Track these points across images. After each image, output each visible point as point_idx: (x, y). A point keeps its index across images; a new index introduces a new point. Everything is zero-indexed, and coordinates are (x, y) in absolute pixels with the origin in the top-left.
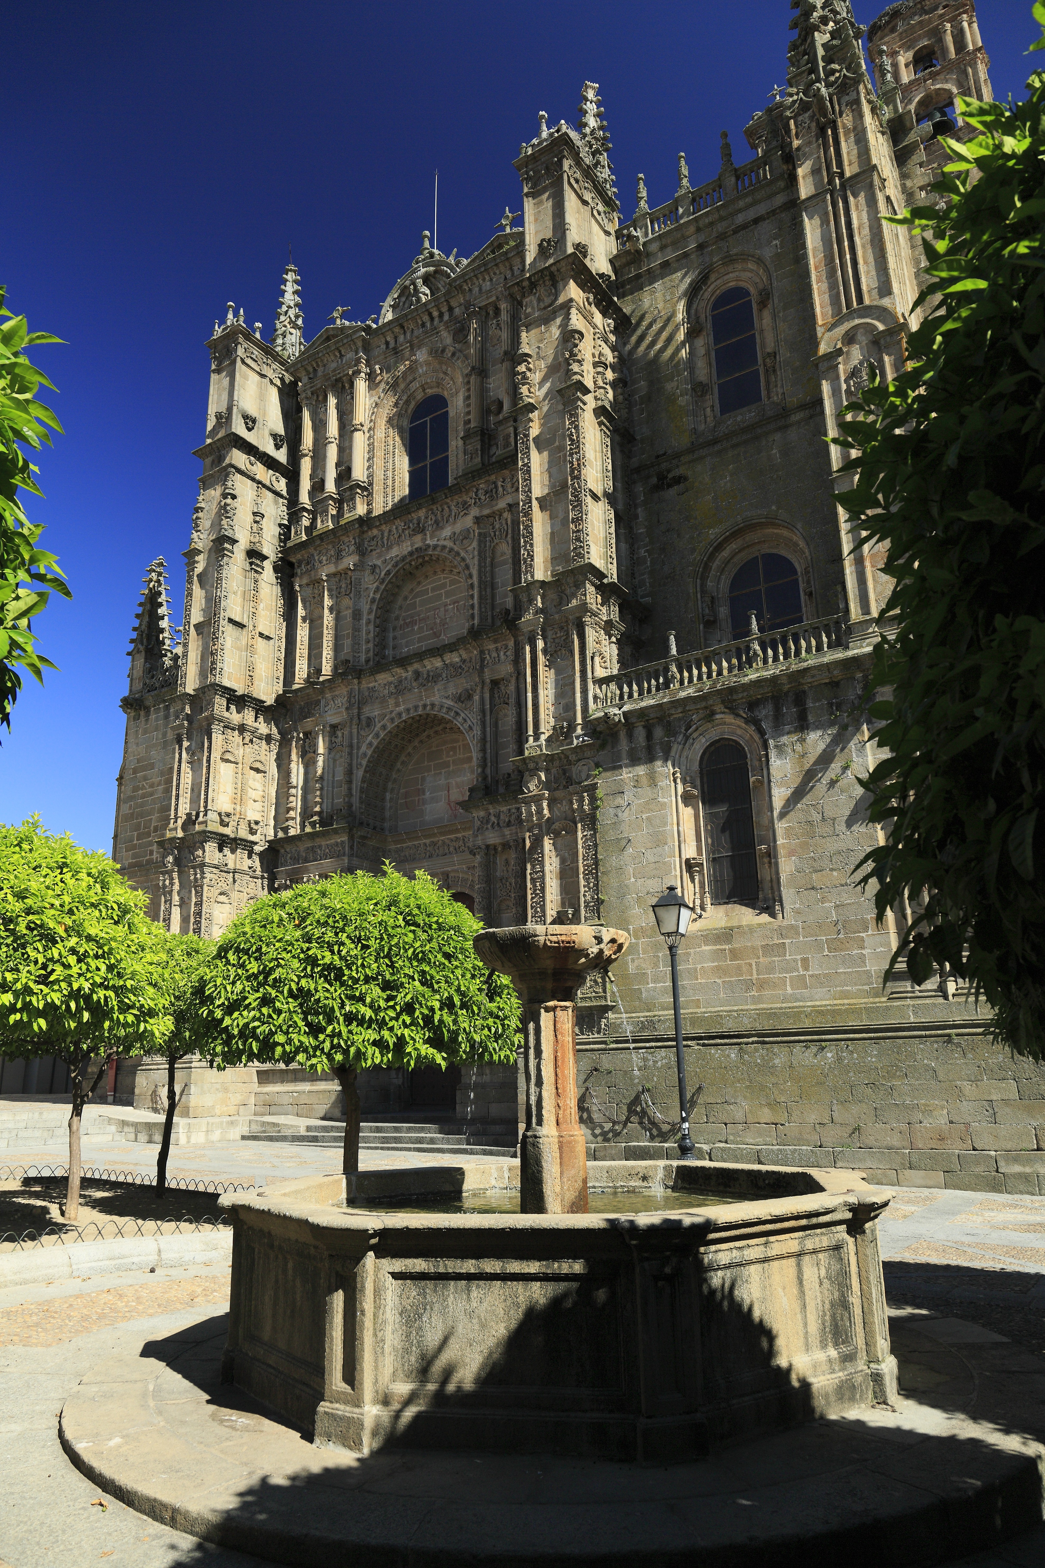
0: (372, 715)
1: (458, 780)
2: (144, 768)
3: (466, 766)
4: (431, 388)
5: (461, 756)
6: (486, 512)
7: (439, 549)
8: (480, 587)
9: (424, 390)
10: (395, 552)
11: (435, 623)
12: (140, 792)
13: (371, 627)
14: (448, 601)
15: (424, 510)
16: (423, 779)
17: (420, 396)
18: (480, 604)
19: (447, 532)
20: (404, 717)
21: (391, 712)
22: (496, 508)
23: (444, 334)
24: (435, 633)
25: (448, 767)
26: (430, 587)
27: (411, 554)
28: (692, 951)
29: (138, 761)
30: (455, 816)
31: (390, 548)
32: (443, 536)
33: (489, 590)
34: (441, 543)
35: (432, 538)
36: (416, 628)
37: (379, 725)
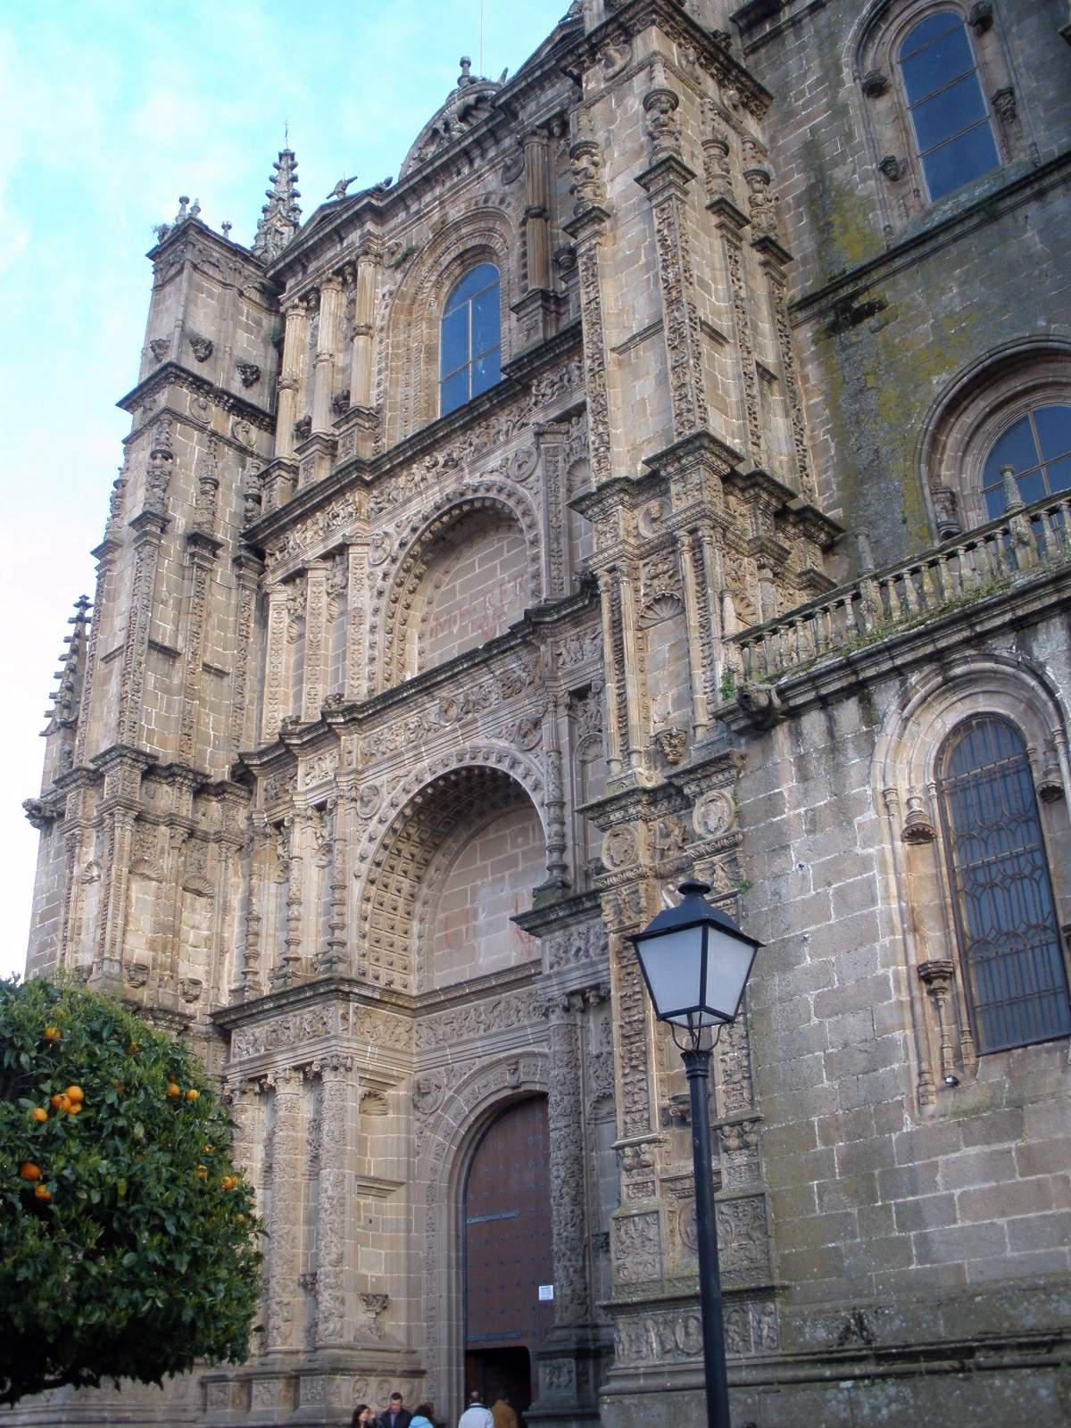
0: (377, 783)
6: (555, 413)
7: (482, 489)
8: (548, 536)
11: (485, 617)
13: (380, 637)
14: (506, 576)
16: (474, 891)
18: (549, 564)
19: (494, 461)
22: (570, 405)
23: (489, 177)
25: (516, 865)
28: (941, 1159)
32: (489, 468)
33: (564, 541)
34: (487, 478)
35: (471, 473)
36: (455, 629)
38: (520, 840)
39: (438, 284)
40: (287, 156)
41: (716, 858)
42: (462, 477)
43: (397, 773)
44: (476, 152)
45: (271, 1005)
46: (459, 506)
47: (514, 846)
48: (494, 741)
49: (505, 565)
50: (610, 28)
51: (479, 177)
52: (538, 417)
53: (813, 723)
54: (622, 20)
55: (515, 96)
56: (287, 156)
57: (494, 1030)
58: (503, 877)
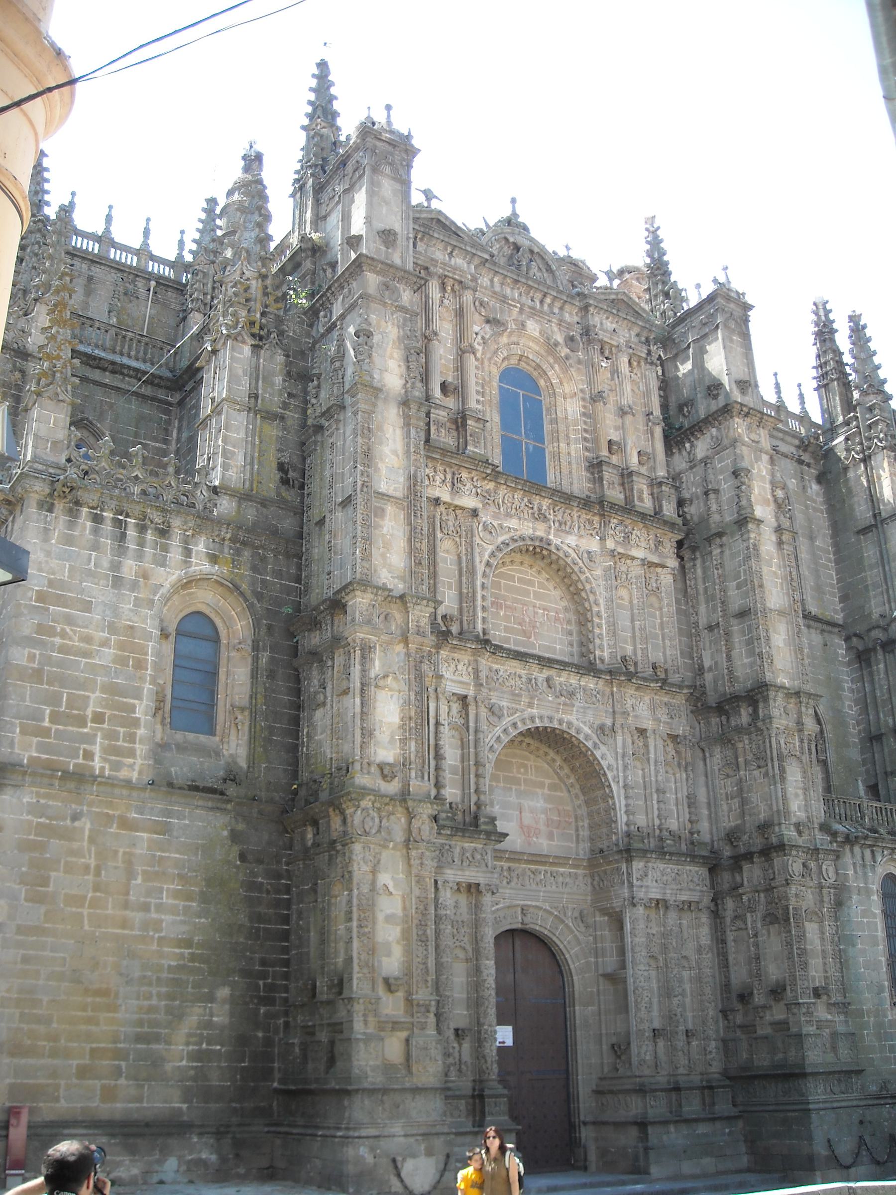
1: (531, 803)
2: (61, 601)
3: (539, 791)
4: (528, 364)
5: (533, 778)
9: (520, 360)
10: (513, 523)
11: (523, 619)
12: (58, 640)
14: (538, 603)
15: (550, 501)
17: (514, 361)
19: (572, 540)
20: (538, 723)
21: (522, 711)
24: (524, 631)
25: (520, 785)
26: (517, 575)
27: (532, 539)
29: (51, 583)
30: (529, 844)
31: (508, 515)
34: (566, 548)
37: (507, 721)
38: (522, 770)
39: (504, 359)
40: (323, 65)
41: (832, 891)
42: (549, 533)
43: (514, 705)
44: (548, 300)
45: (449, 833)
46: (542, 548)
47: (518, 772)
48: (581, 725)
49: (537, 595)
50: (759, 415)
51: (549, 321)
52: (610, 544)
53: (857, 849)
54: (765, 417)
55: (596, 307)
56: (323, 65)
57: (513, 884)
58: (511, 789)
